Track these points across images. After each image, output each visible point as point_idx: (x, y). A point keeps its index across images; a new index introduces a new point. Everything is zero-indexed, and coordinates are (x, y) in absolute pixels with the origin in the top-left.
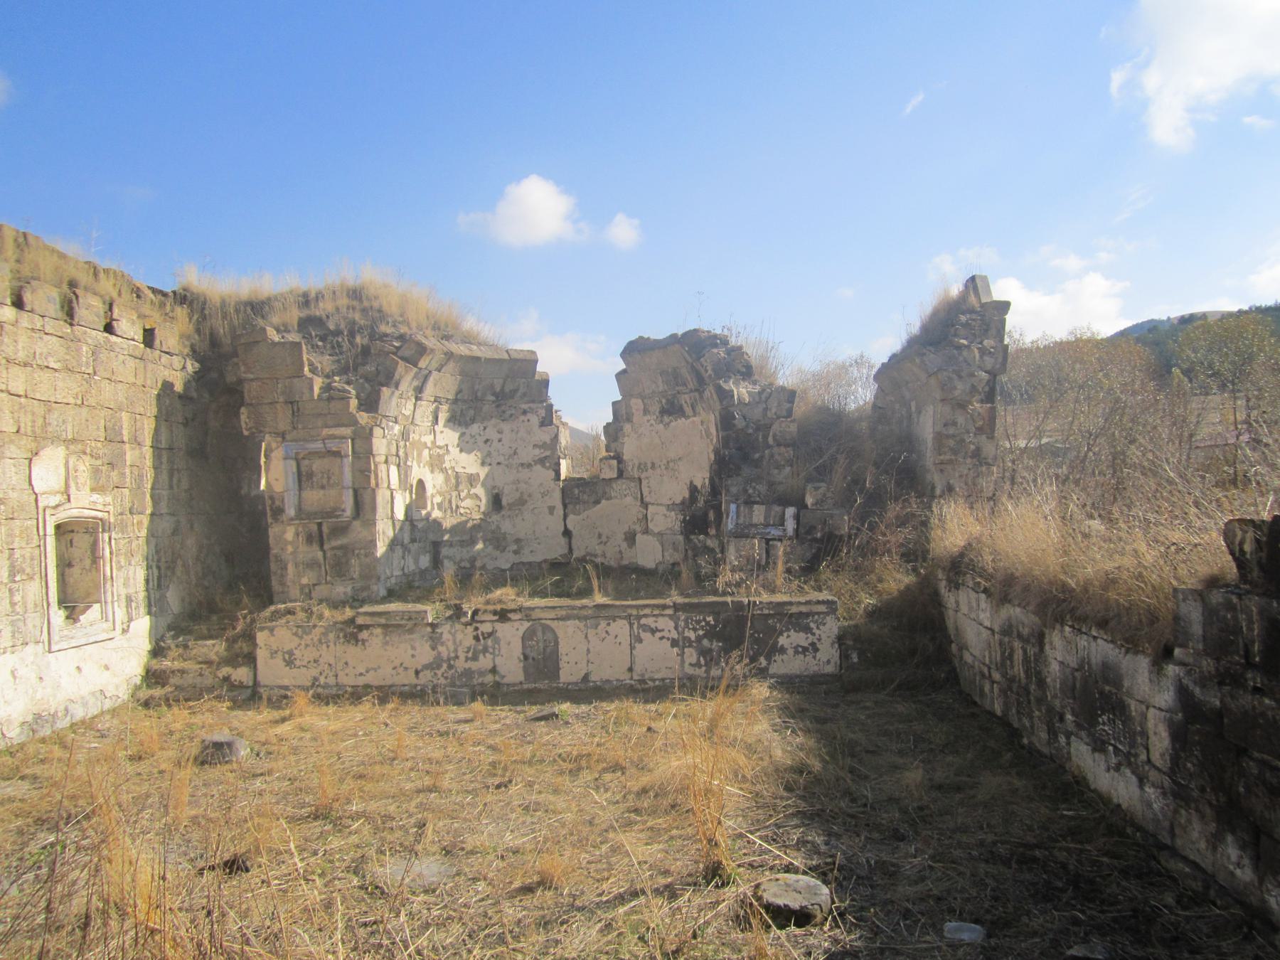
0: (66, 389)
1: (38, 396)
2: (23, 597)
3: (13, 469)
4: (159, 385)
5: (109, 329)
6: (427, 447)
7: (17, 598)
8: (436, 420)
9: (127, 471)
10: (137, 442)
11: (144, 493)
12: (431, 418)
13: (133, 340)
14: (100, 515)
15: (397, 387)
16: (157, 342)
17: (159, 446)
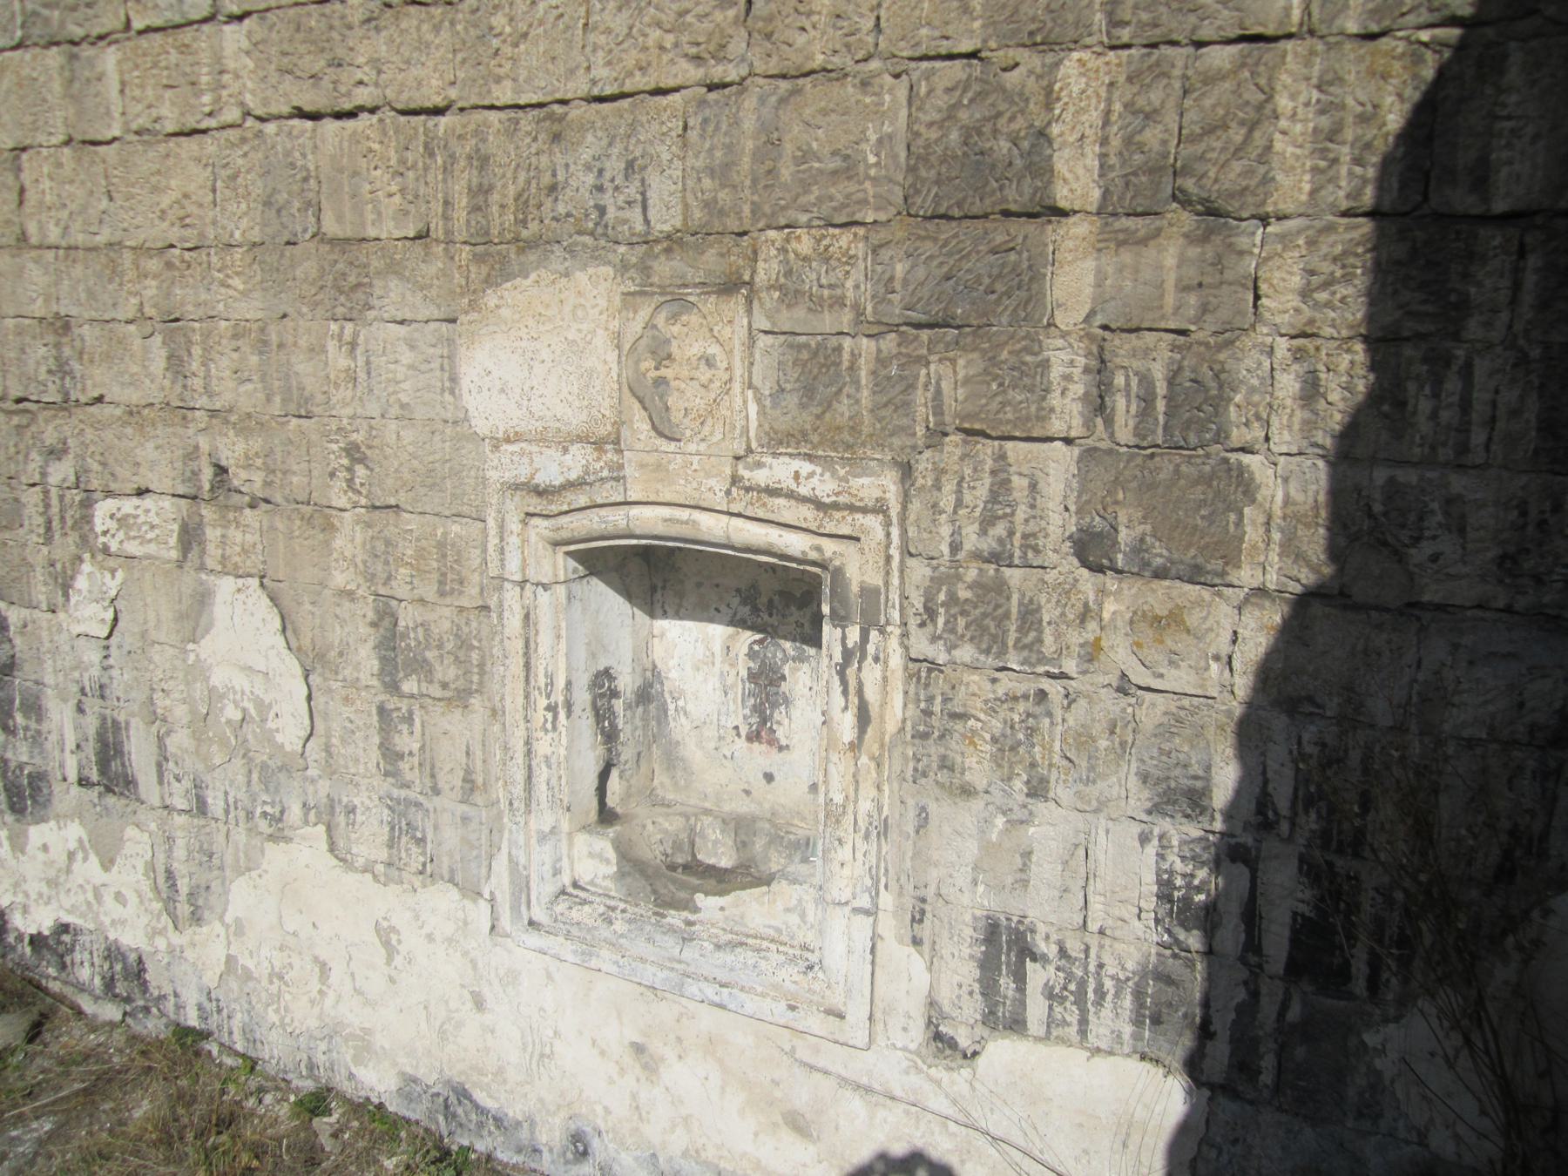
1: (504, 94)
2: (422, 748)
3: (407, 357)
7: (406, 741)
14: (796, 544)
17: (1462, 200)
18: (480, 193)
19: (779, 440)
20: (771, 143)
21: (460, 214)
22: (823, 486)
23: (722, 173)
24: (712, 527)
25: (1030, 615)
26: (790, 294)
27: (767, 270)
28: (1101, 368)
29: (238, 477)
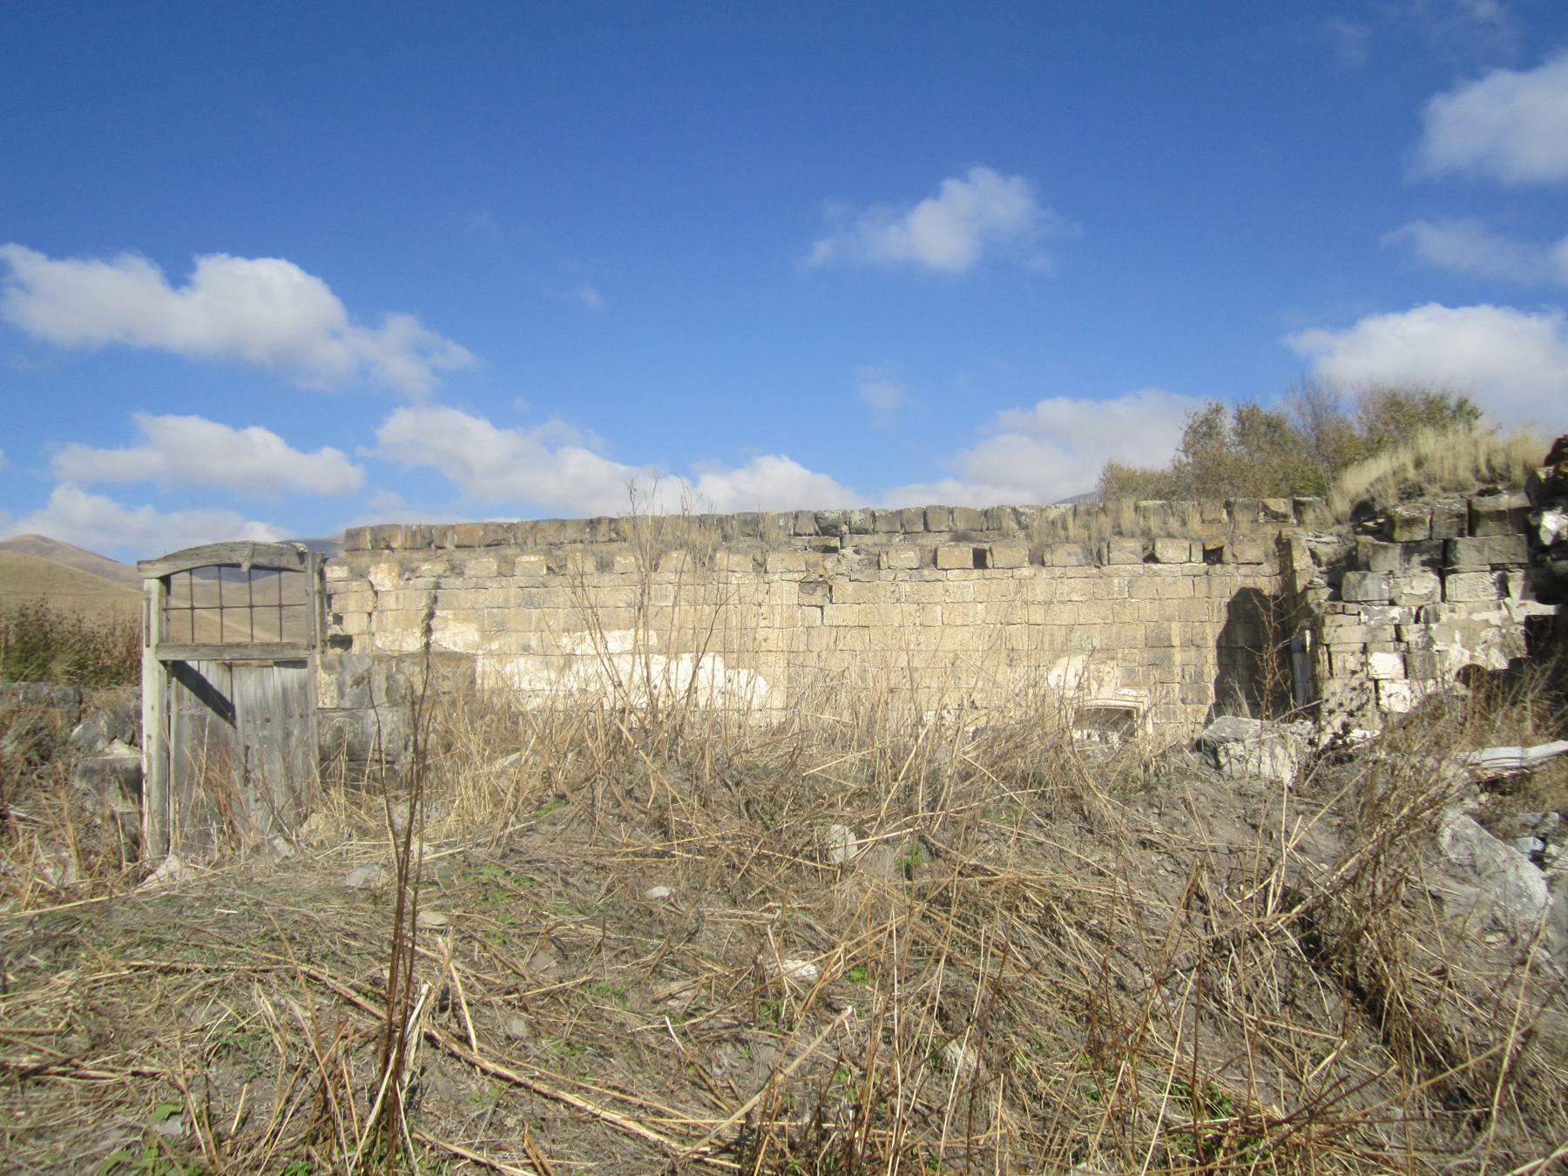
0: (1086, 615)
4: (1234, 593)
5: (1151, 558)
6: (1491, 626)
8: (1504, 590)
9: (1177, 670)
10: (1191, 643)
11: (1204, 690)
12: (1494, 590)
13: (1190, 561)
15: (1369, 569)
16: (1227, 556)
18: (1052, 642)
19: (1124, 686)
20: (1119, 634)
21: (1047, 646)
22: (1135, 693)
23: (1109, 638)
24: (1113, 703)
25: (1174, 713)
26: (1124, 660)
27: (1120, 656)
28: (1183, 670)
29: (978, 703)
